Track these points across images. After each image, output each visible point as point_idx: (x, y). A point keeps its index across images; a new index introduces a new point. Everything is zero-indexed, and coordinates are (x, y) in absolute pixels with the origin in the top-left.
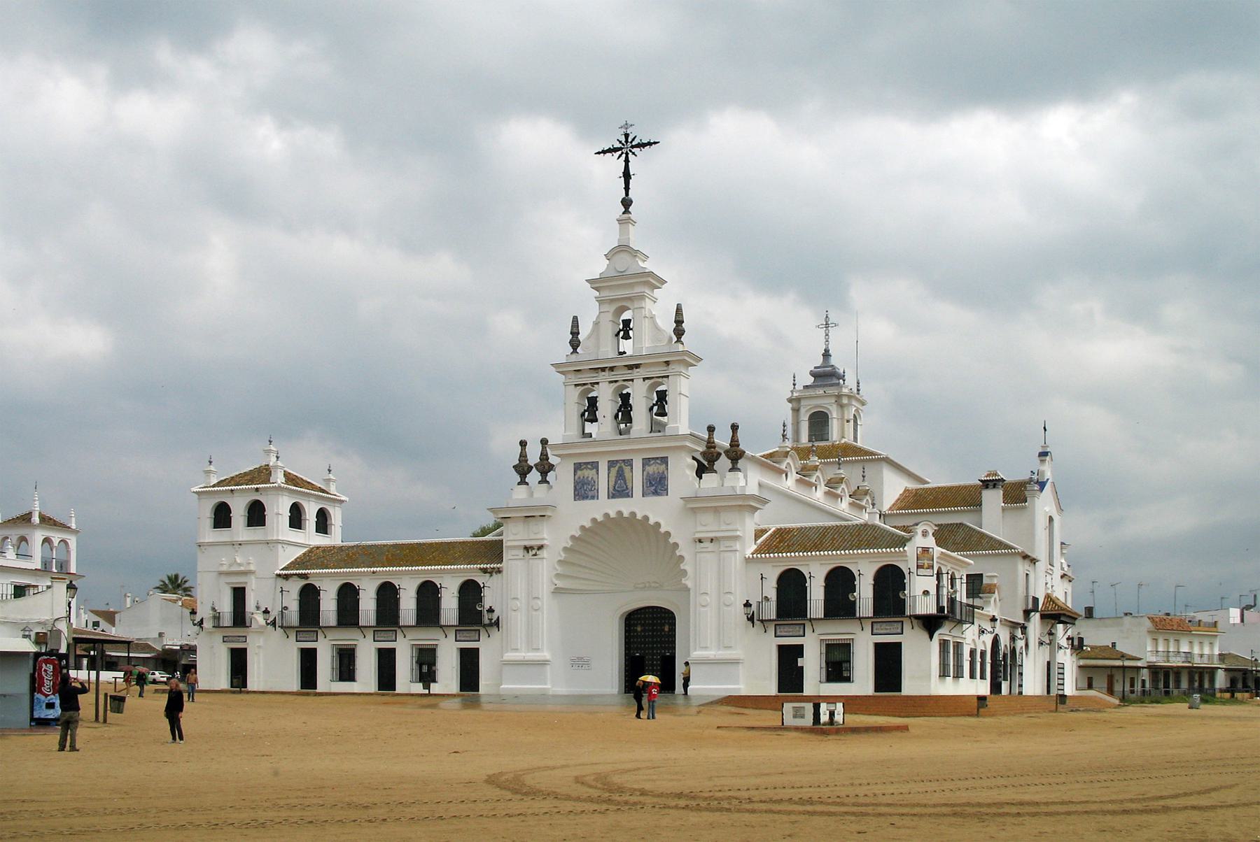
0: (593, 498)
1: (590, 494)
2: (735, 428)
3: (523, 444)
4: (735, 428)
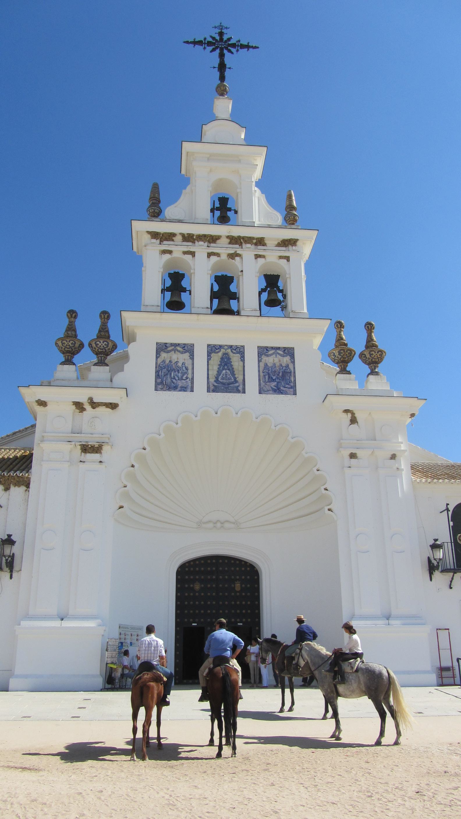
0: (184, 389)
1: (180, 384)
2: (369, 327)
3: (72, 314)
4: (369, 327)
